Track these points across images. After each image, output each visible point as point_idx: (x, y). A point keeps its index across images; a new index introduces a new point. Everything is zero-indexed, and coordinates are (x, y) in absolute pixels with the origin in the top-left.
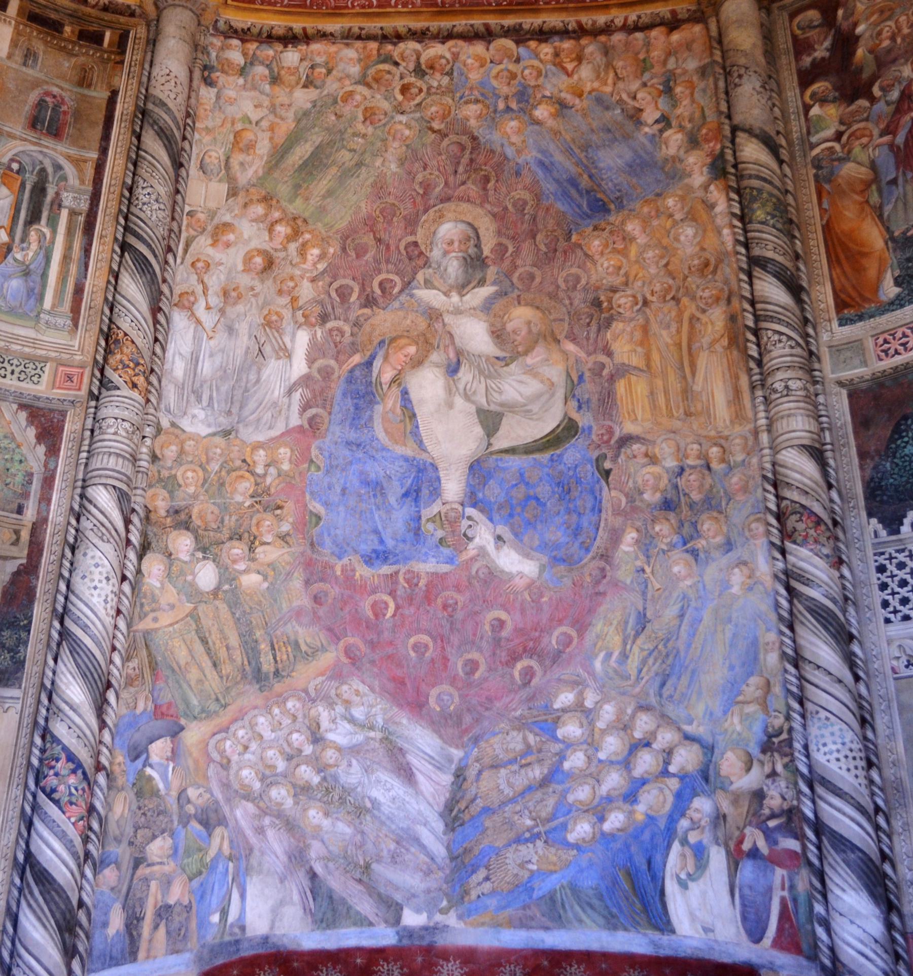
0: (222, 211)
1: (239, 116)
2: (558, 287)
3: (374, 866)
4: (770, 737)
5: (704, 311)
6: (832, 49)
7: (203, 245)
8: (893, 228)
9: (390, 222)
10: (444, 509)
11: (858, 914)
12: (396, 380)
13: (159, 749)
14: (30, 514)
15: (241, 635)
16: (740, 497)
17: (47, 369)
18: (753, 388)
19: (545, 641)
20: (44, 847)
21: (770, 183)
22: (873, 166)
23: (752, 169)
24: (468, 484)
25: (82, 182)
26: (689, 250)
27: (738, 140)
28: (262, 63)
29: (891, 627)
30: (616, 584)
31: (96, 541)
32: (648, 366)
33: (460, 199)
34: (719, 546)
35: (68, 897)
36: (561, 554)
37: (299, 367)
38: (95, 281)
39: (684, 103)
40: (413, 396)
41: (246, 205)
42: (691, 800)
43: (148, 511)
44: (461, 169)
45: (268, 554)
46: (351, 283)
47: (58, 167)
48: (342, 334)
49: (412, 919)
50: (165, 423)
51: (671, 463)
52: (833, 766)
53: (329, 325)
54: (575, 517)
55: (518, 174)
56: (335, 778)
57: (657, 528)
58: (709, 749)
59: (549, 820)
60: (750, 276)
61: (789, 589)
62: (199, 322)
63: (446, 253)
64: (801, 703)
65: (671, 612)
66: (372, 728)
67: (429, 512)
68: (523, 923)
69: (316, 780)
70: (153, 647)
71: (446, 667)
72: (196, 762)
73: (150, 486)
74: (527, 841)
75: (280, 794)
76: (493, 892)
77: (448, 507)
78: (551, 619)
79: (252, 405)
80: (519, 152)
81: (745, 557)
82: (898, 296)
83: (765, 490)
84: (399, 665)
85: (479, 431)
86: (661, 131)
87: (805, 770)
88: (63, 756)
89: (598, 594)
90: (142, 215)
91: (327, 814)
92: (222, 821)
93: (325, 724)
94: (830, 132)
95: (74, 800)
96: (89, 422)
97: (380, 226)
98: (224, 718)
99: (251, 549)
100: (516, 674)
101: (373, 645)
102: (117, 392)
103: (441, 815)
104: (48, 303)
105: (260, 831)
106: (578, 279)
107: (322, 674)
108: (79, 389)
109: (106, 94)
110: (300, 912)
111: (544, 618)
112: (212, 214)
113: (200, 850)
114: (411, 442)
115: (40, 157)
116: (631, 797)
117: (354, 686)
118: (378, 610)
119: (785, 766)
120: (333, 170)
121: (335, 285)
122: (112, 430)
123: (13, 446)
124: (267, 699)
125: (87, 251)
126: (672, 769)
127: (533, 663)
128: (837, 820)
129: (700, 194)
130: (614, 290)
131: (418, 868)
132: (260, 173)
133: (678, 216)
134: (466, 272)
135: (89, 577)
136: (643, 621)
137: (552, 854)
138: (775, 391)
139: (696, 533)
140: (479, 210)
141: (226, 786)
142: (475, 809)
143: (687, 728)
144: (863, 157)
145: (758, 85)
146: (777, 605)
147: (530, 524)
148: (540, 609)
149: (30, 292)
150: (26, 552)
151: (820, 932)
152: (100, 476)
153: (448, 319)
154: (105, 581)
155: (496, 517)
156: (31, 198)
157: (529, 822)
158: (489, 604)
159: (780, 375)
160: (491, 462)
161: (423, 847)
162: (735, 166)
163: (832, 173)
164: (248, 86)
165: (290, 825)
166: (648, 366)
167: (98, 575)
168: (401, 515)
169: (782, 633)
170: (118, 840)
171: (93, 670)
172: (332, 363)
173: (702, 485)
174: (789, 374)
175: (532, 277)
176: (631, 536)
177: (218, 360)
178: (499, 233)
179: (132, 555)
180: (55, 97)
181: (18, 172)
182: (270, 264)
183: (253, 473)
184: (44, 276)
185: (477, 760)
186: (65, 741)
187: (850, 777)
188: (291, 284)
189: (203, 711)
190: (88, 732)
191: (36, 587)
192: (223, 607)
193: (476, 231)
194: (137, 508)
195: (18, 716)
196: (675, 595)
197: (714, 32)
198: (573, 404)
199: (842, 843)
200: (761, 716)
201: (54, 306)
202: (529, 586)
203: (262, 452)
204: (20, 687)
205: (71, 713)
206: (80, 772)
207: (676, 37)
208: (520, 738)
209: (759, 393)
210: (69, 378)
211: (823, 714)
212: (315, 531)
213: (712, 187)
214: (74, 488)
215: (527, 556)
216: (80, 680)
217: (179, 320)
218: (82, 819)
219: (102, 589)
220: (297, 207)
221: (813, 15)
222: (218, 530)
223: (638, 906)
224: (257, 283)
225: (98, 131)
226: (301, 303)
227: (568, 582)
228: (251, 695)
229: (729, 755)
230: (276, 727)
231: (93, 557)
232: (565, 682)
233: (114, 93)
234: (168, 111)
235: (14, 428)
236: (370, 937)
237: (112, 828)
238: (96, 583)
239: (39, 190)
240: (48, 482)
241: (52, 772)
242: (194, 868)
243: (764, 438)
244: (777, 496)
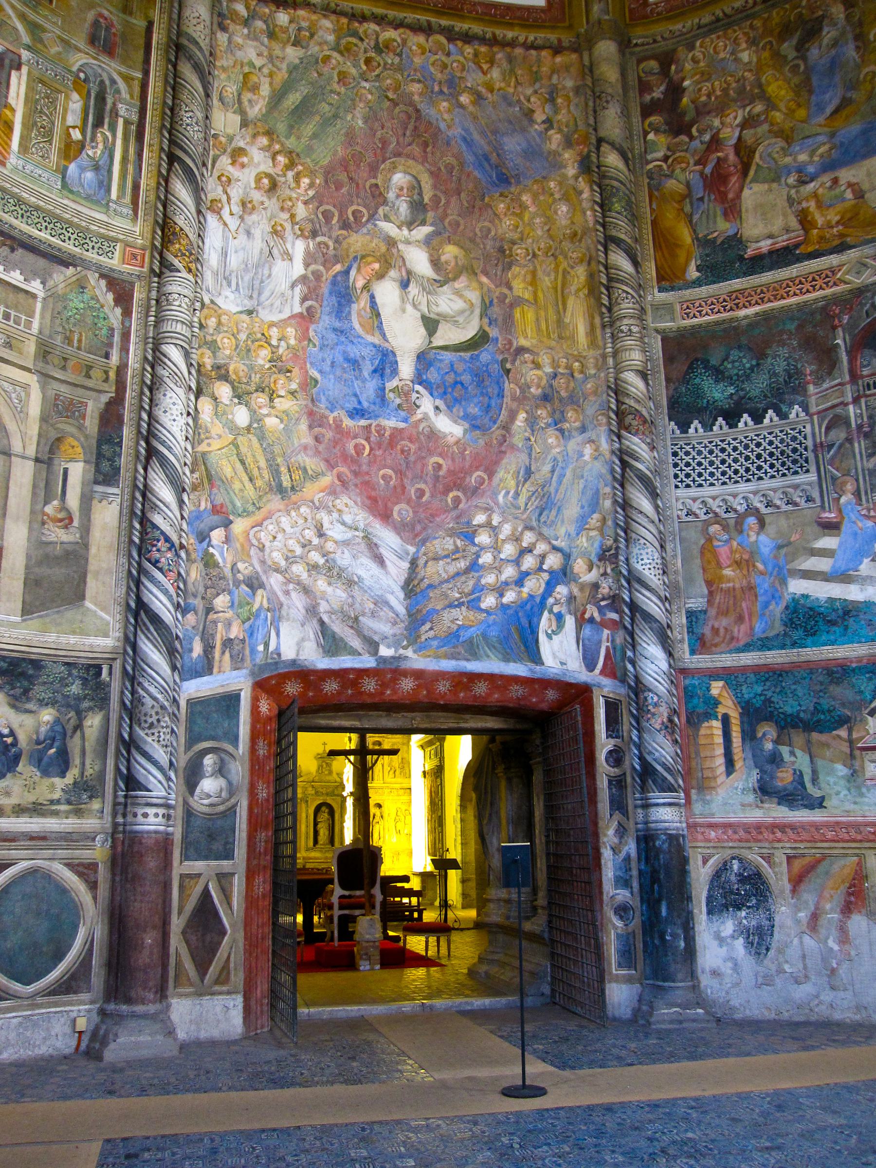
0: (238, 138)
1: (245, 61)
2: (476, 235)
3: (361, 618)
4: (604, 551)
5: (572, 268)
6: (665, 93)
7: (224, 161)
8: (698, 231)
9: (358, 166)
10: (400, 384)
11: (656, 658)
12: (366, 287)
13: (217, 535)
14: (115, 359)
15: (267, 460)
16: (592, 398)
17: (117, 248)
18: (604, 327)
19: (468, 480)
21: (625, 185)
22: (688, 185)
23: (613, 172)
24: (417, 369)
25: (132, 97)
26: (564, 222)
27: (602, 149)
28: (261, 19)
29: (678, 491)
30: (513, 447)
31: (172, 385)
32: (535, 300)
33: (408, 156)
34: (577, 429)
36: (478, 422)
37: (298, 269)
38: (147, 181)
39: (563, 111)
40: (378, 300)
41: (254, 136)
42: (555, 587)
43: (199, 365)
44: (408, 133)
45: (284, 404)
46: (332, 209)
47: (113, 82)
48: (328, 247)
49: (385, 651)
50: (207, 301)
51: (548, 370)
52: (647, 572)
53: (319, 239)
54: (486, 399)
55: (448, 144)
56: (334, 561)
57: (539, 412)
58: (567, 556)
59: (470, 595)
60: (606, 250)
61: (622, 461)
62: (225, 224)
63: (398, 196)
64: (626, 533)
65: (547, 468)
66: (356, 529)
67: (391, 385)
68: (454, 657)
69: (321, 561)
70: (209, 465)
71: (404, 492)
72: (242, 546)
73: (200, 347)
74: (456, 606)
75: (298, 569)
76: (435, 638)
77: (403, 383)
78: (471, 466)
79: (266, 294)
80: (449, 127)
81: (594, 437)
82: (698, 279)
83: (609, 395)
84: (374, 489)
85: (423, 331)
86: (547, 130)
87: (626, 573)
88: (162, 538)
89: (502, 452)
90: (186, 134)
91: (330, 584)
92: (262, 586)
93: (326, 525)
94: (660, 155)
96: (154, 294)
97: (352, 168)
98: (258, 516)
99: (271, 400)
100: (449, 500)
101: (356, 474)
102: (179, 274)
103: (403, 588)
104: (114, 195)
105: (287, 593)
106: (489, 230)
107: (322, 491)
108: (142, 267)
109: (143, 24)
110: (315, 646)
111: (467, 464)
112: (231, 139)
113: (248, 604)
114: (377, 333)
115: (100, 71)
116: (519, 582)
117: (343, 501)
118: (359, 449)
119: (612, 570)
120: (317, 118)
121: (321, 209)
122: (177, 303)
124: (287, 506)
125: (140, 155)
126: (545, 567)
127: (460, 494)
128: (647, 604)
129: (571, 182)
130: (514, 243)
131: (388, 621)
132: (264, 111)
133: (557, 196)
134: (412, 213)
136: (529, 473)
137: (471, 615)
138: (622, 332)
139: (563, 419)
140: (420, 167)
141: (263, 562)
142: (424, 585)
143: (554, 542)
144: (682, 177)
145: (619, 111)
146: (612, 471)
147: (457, 401)
148: (464, 459)
149: (101, 184)
151: (630, 667)
152: (171, 337)
153: (401, 246)
155: (435, 394)
156: (95, 105)
157: (457, 595)
158: (431, 453)
159: (626, 321)
160: (431, 355)
161: (391, 608)
162: (598, 167)
163: (659, 184)
164: (252, 36)
165: (306, 590)
166: (535, 300)
168: (372, 385)
169: (614, 488)
170: (195, 596)
172: (321, 268)
173: (567, 387)
174: (631, 321)
175: (458, 224)
176: (522, 416)
177: (241, 254)
178: (435, 187)
179: (192, 398)
180: (106, 19)
181: (85, 81)
182: (274, 186)
183: (270, 345)
184: (110, 172)
185: (425, 554)
187: (655, 579)
188: (290, 204)
189: (245, 511)
192: (255, 440)
193: (419, 182)
196: (549, 457)
197: (586, 62)
198: (486, 320)
199: (648, 617)
200: (599, 538)
201: (118, 197)
202: (457, 442)
203: (275, 329)
205: (164, 508)
207: (558, 59)
208: (451, 542)
209: (608, 330)
210: (134, 256)
211: (642, 541)
212: (314, 391)
213: (580, 179)
214: (146, 344)
215: (455, 422)
217: (212, 220)
220: (291, 143)
221: (653, 64)
222: (247, 384)
223: (523, 648)
224: (265, 199)
225: (140, 56)
226: (298, 219)
227: (481, 442)
228: (275, 502)
229: (579, 560)
230: (294, 525)
232: (481, 508)
233: (150, 24)
234: (200, 49)
235: (98, 292)
236: (360, 662)
237: (190, 586)
239: (101, 99)
240: (126, 336)
242: (246, 615)
243: (610, 361)
244: (617, 400)
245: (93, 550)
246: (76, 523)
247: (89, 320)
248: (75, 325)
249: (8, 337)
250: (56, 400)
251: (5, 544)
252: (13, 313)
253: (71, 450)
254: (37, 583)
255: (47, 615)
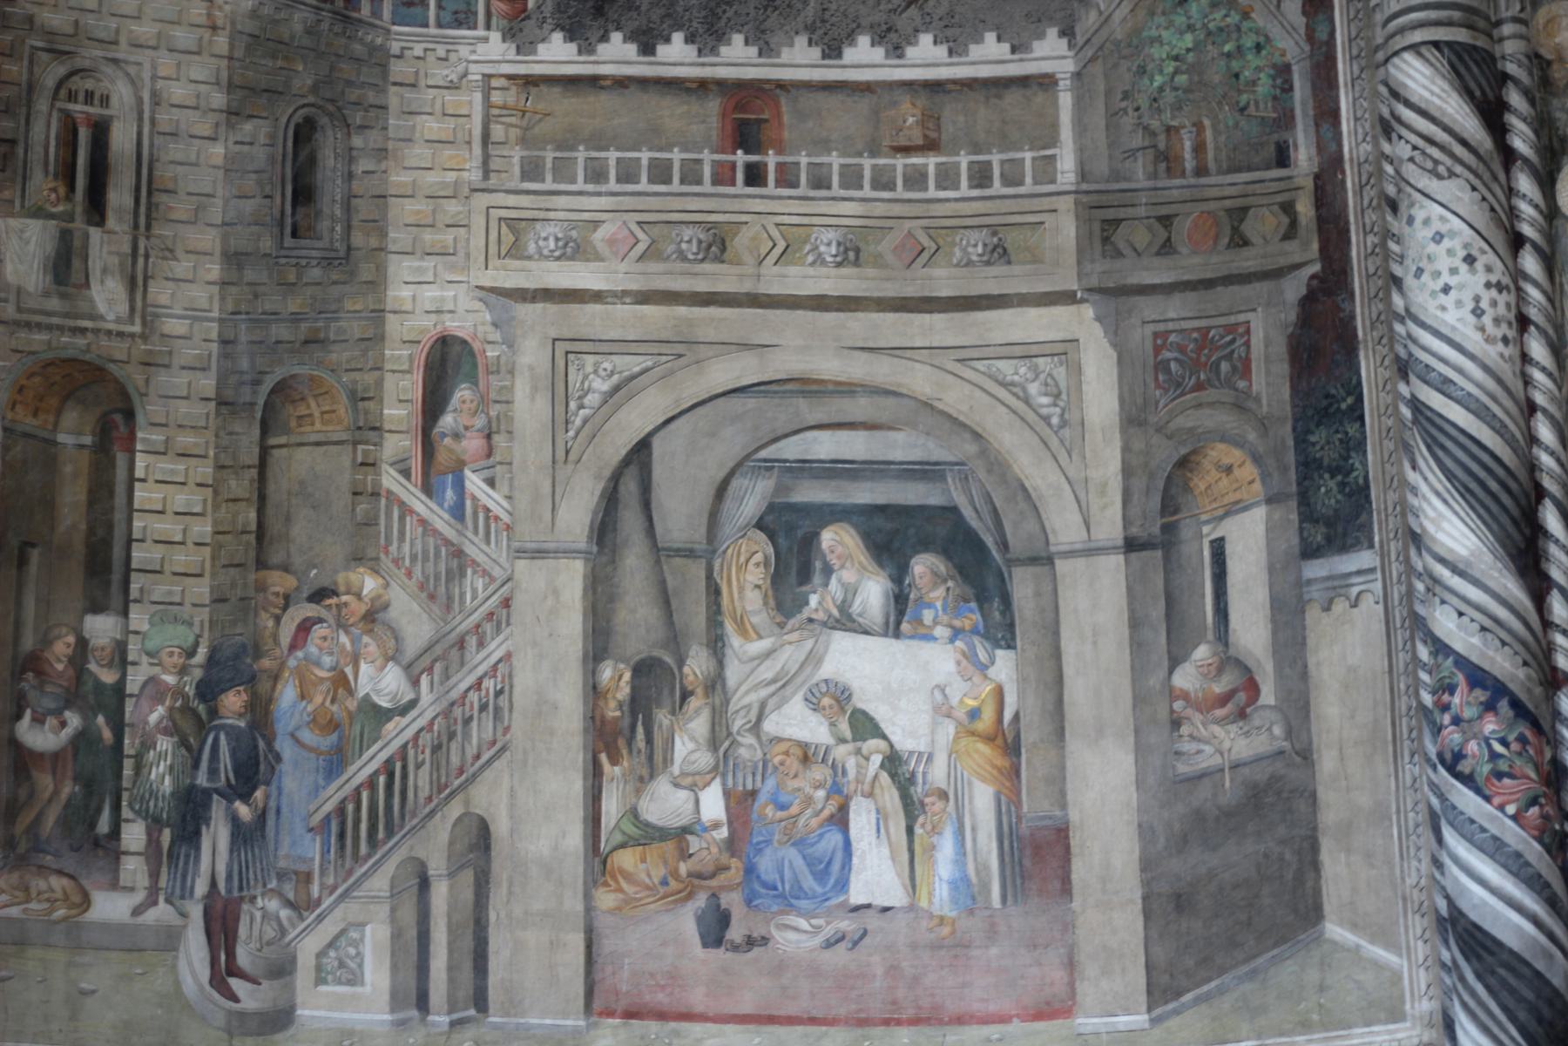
14: (1304, 157)
20: (1464, 879)
31: (1425, 182)
35: (1538, 974)
88: (1460, 678)
95: (1503, 766)
123: (1234, 18)
135: (1428, 268)
150: (1315, 246)
152: (1401, 31)
154: (1464, 268)
167: (1445, 258)
171: (1482, 474)
179: (1525, 183)
186: (1458, 646)
190: (1502, 613)
191: (1352, 317)
194: (1511, 68)
195: (1380, 607)
204: (1371, 546)
205: (1456, 582)
206: (1504, 705)
216: (1460, 505)
218: (1534, 802)
219: (1461, 287)
231: (1427, 222)
238: (1446, 278)
241: (1447, 719)
245: (1327, 763)
246: (1268, 696)
247: (1216, 75)
248: (1177, 107)
249: (994, 229)
250: (1157, 350)
251: (1074, 815)
252: (995, 158)
253: (1225, 481)
254: (1181, 902)
255: (1221, 991)
